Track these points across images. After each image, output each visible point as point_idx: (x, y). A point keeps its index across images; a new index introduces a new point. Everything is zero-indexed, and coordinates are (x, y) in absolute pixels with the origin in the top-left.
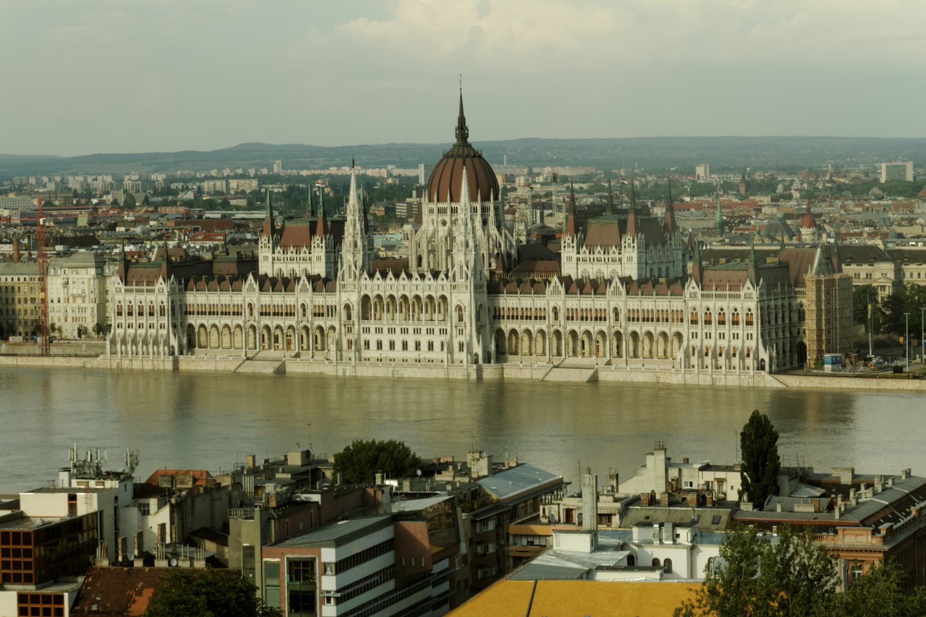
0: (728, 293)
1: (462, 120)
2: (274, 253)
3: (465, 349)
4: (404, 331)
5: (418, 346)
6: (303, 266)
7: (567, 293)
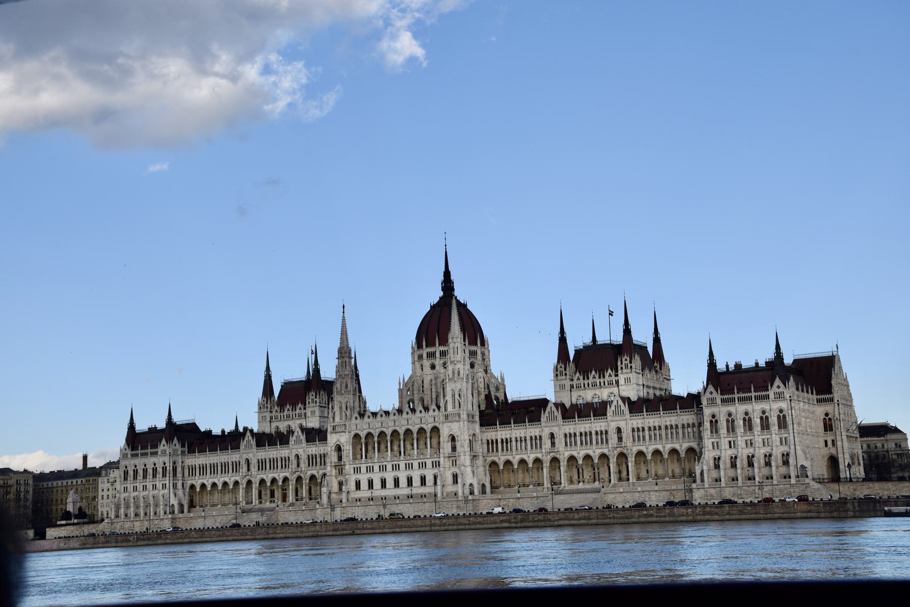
0: (753, 394)
1: (447, 274)
2: (271, 412)
3: (459, 480)
4: (396, 467)
6: (298, 422)
7: (564, 418)
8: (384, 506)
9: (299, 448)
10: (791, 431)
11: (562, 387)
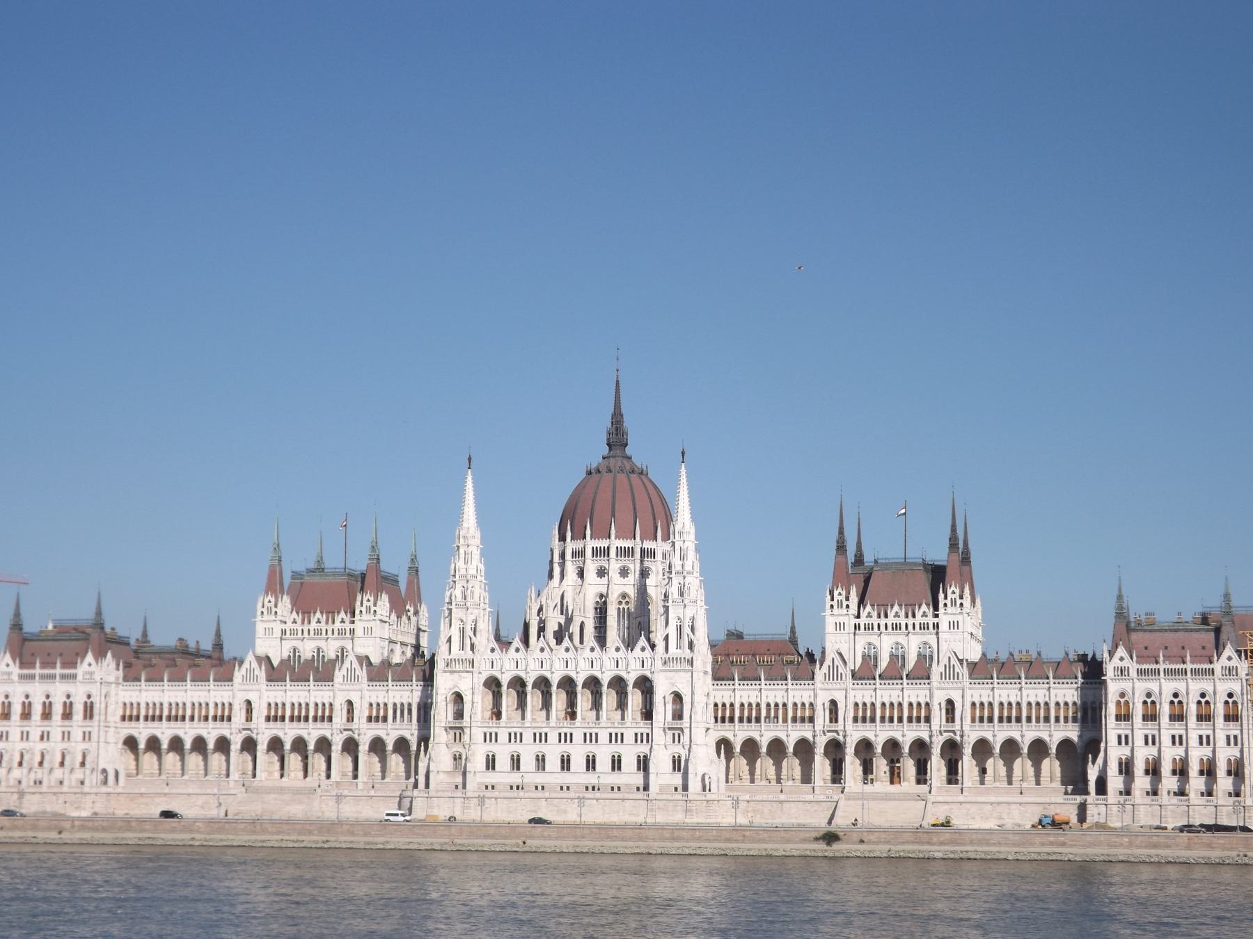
0: (1189, 666)
1: (617, 418)
4: (566, 738)
5: (591, 763)
6: (338, 644)
8: (581, 800)
9: (351, 690)
10: (1245, 726)
11: (840, 626)
